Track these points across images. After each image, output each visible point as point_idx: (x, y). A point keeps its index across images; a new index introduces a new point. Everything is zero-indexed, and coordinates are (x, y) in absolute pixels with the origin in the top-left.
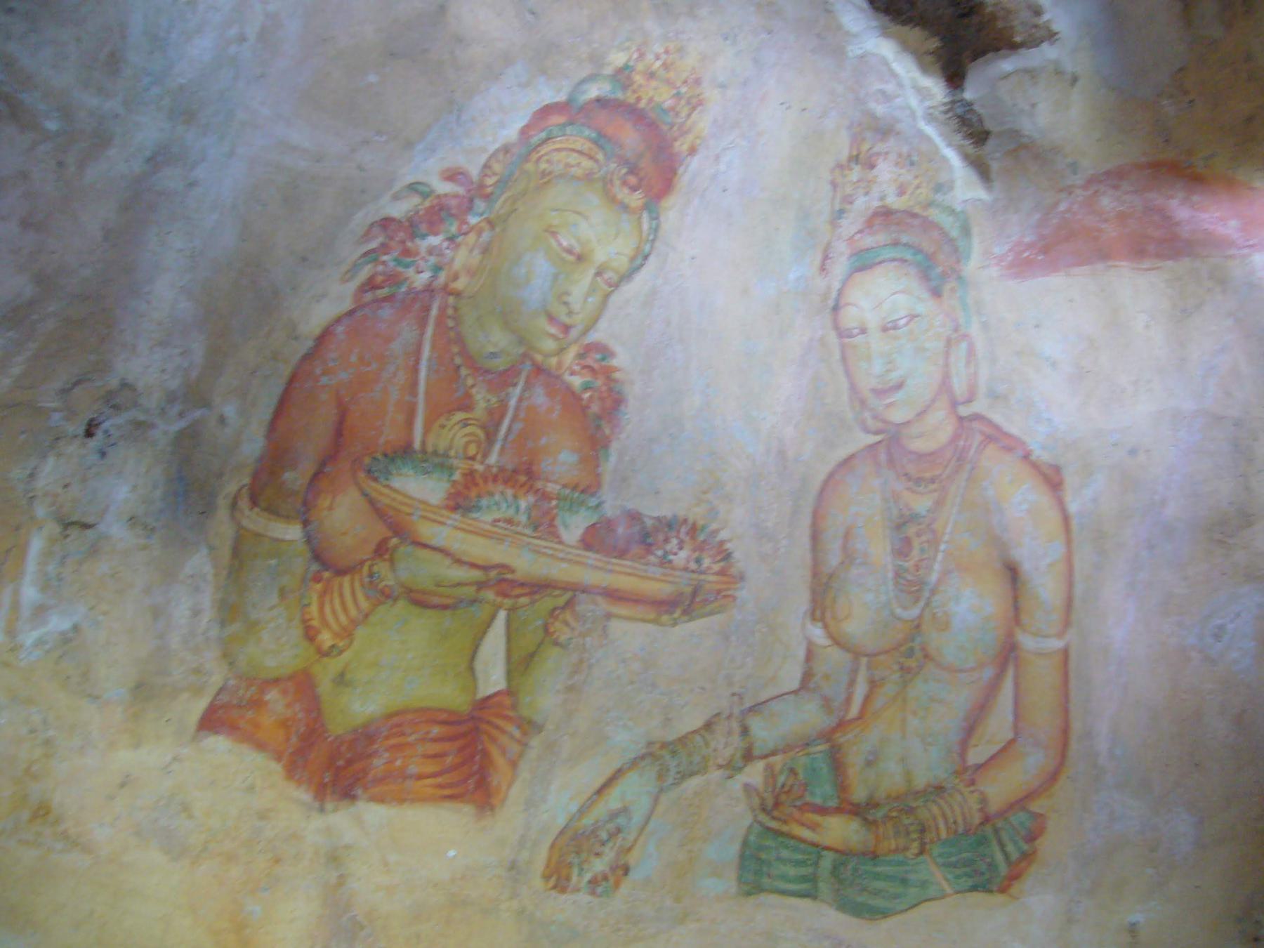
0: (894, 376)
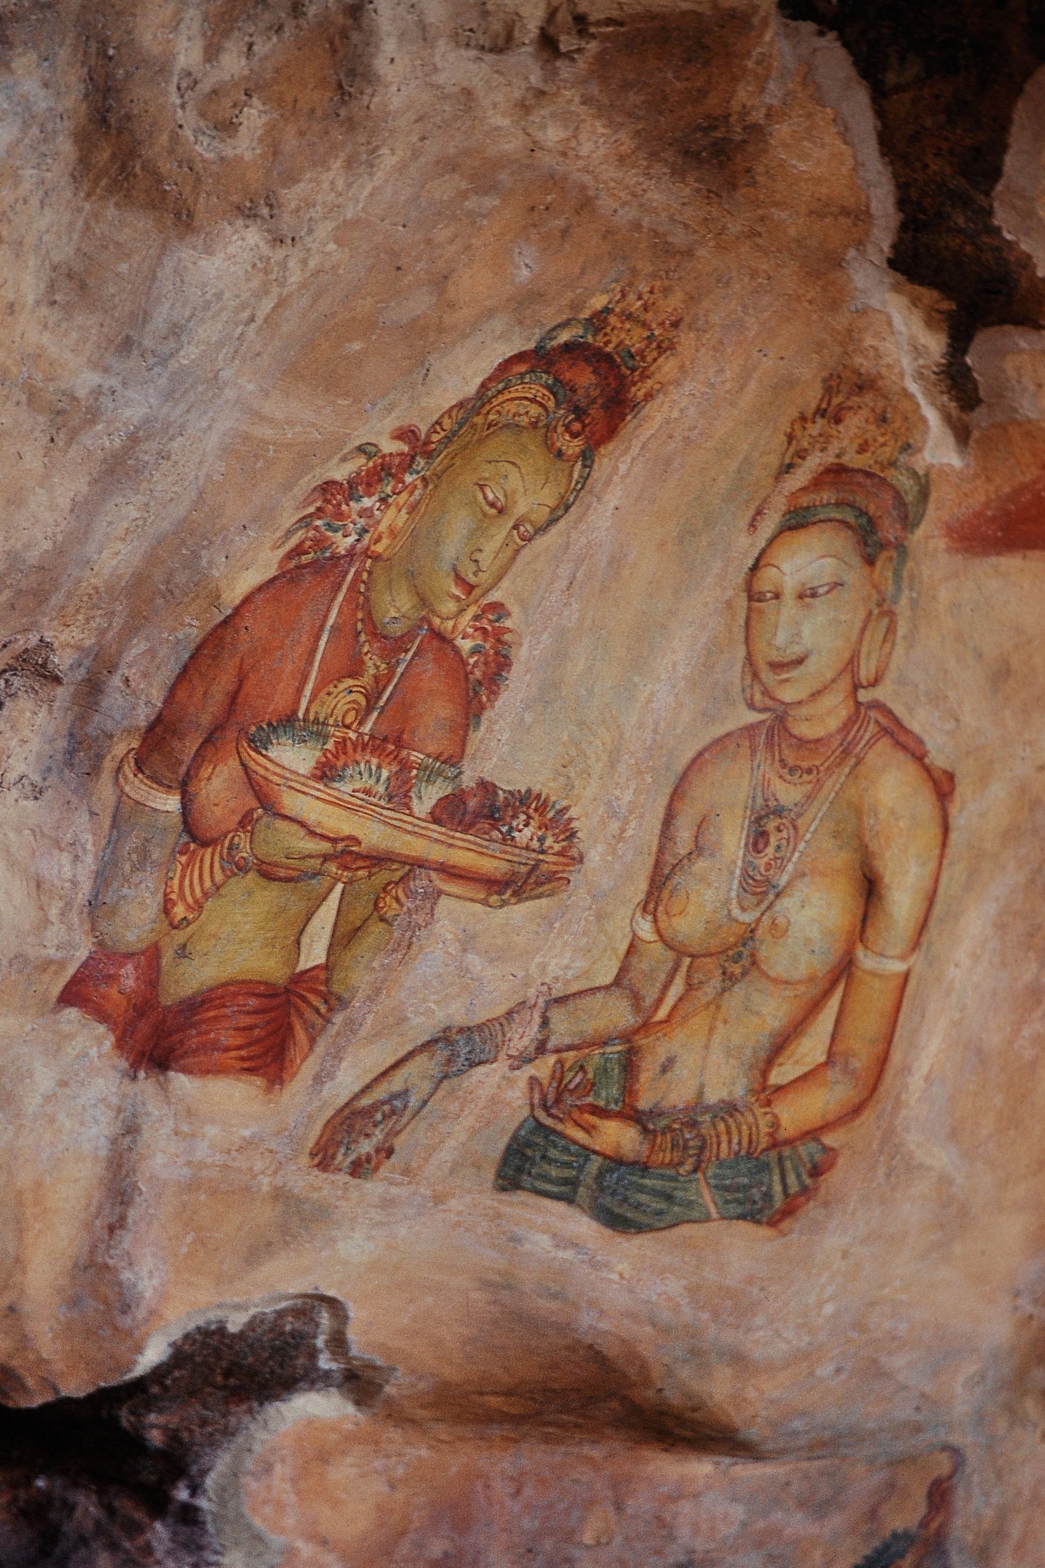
0: (796, 650)
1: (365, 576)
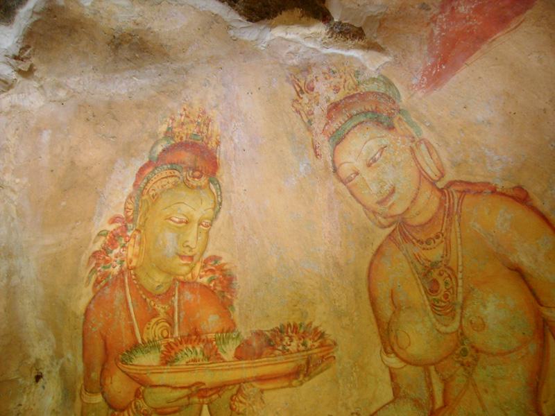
0: (387, 188)
1: (133, 277)
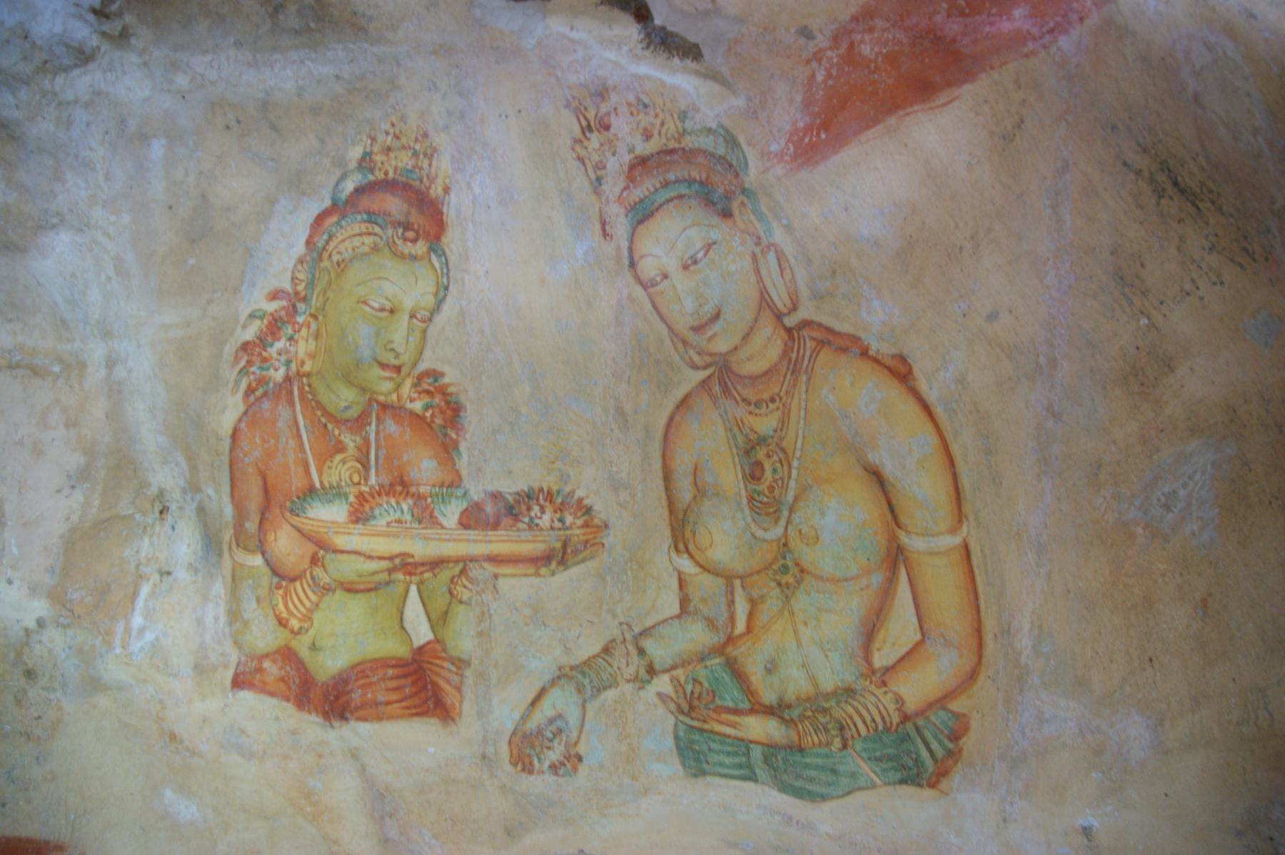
0: (708, 309)
1: (307, 388)
